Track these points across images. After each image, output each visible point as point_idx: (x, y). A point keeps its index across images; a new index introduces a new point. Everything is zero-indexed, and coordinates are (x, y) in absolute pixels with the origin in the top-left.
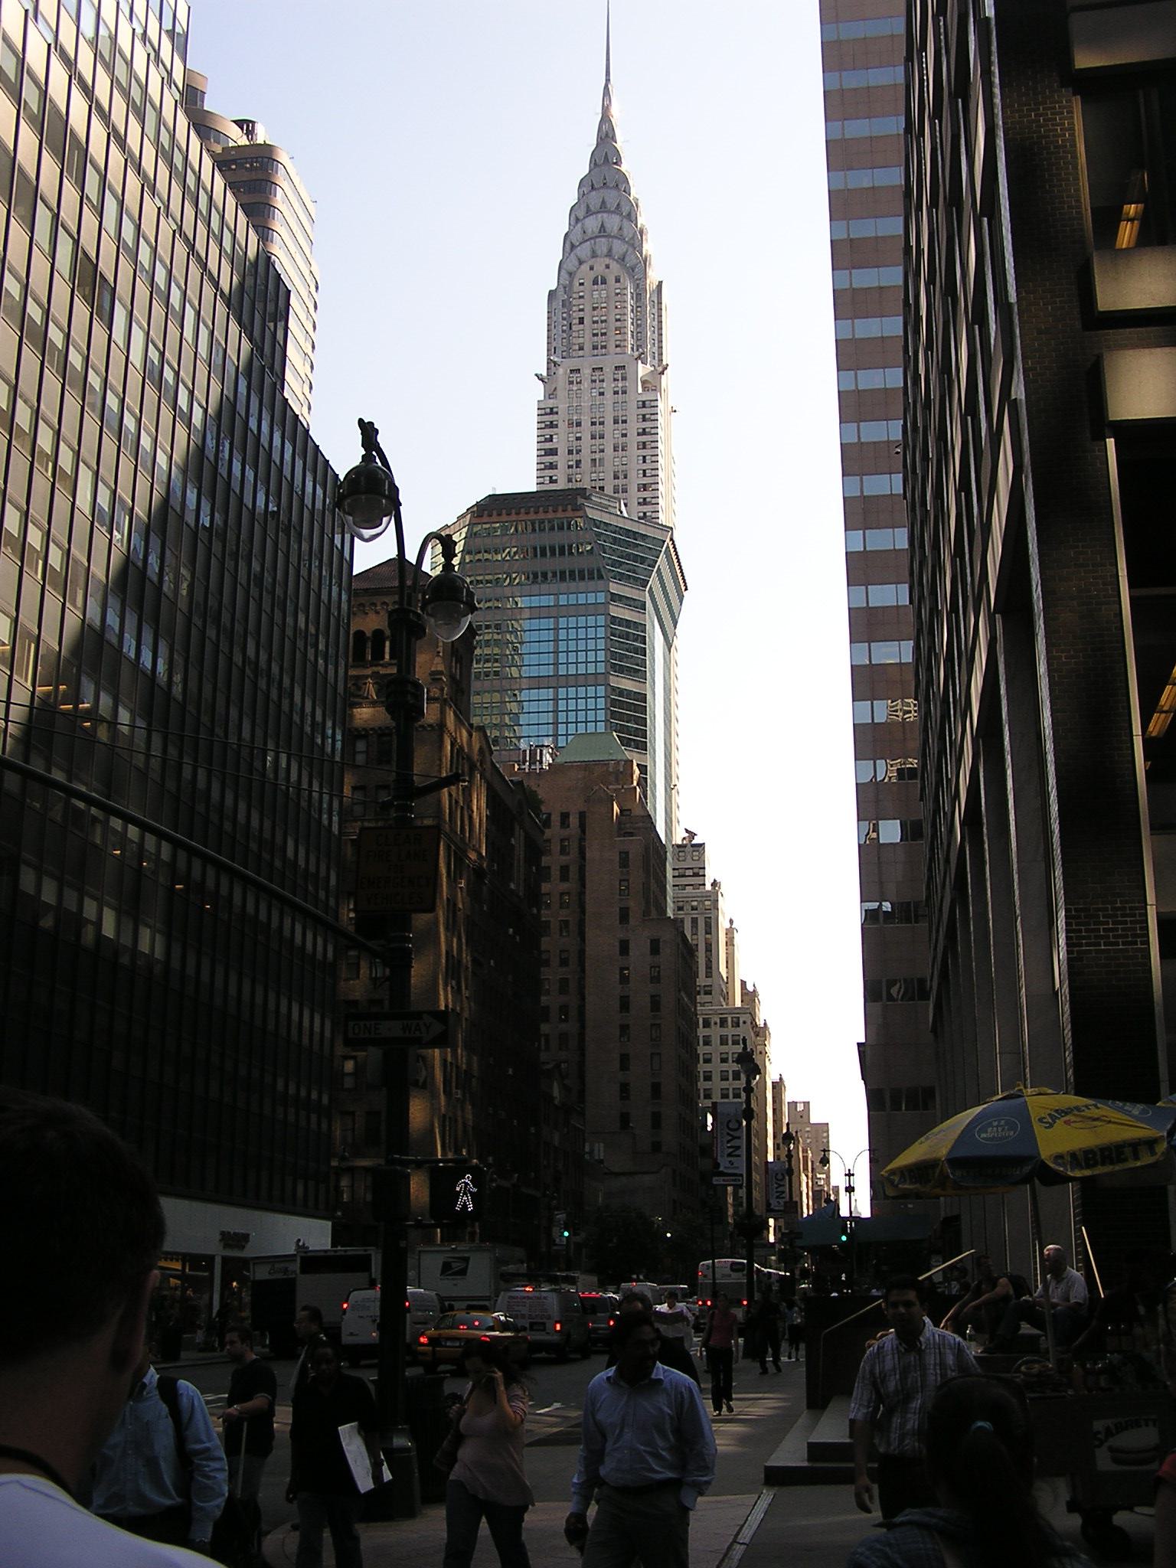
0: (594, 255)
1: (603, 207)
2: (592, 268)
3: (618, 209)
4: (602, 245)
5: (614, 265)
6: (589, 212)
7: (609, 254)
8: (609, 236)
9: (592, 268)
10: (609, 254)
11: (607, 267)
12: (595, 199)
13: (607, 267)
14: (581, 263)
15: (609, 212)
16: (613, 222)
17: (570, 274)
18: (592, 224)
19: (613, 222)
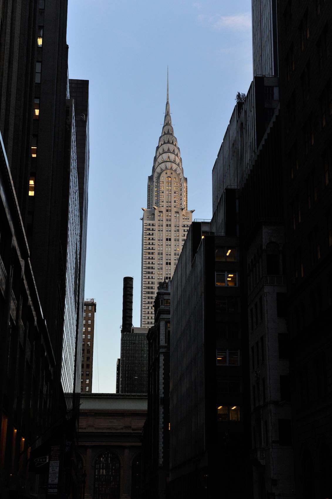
1: (169, 151)
2: (166, 173)
3: (173, 153)
4: (169, 165)
6: (164, 152)
8: (171, 162)
9: (166, 173)
10: (171, 169)
11: (172, 173)
12: (166, 147)
13: (172, 173)
14: (162, 171)
15: (170, 152)
17: (158, 173)
18: (165, 156)
19: (172, 157)
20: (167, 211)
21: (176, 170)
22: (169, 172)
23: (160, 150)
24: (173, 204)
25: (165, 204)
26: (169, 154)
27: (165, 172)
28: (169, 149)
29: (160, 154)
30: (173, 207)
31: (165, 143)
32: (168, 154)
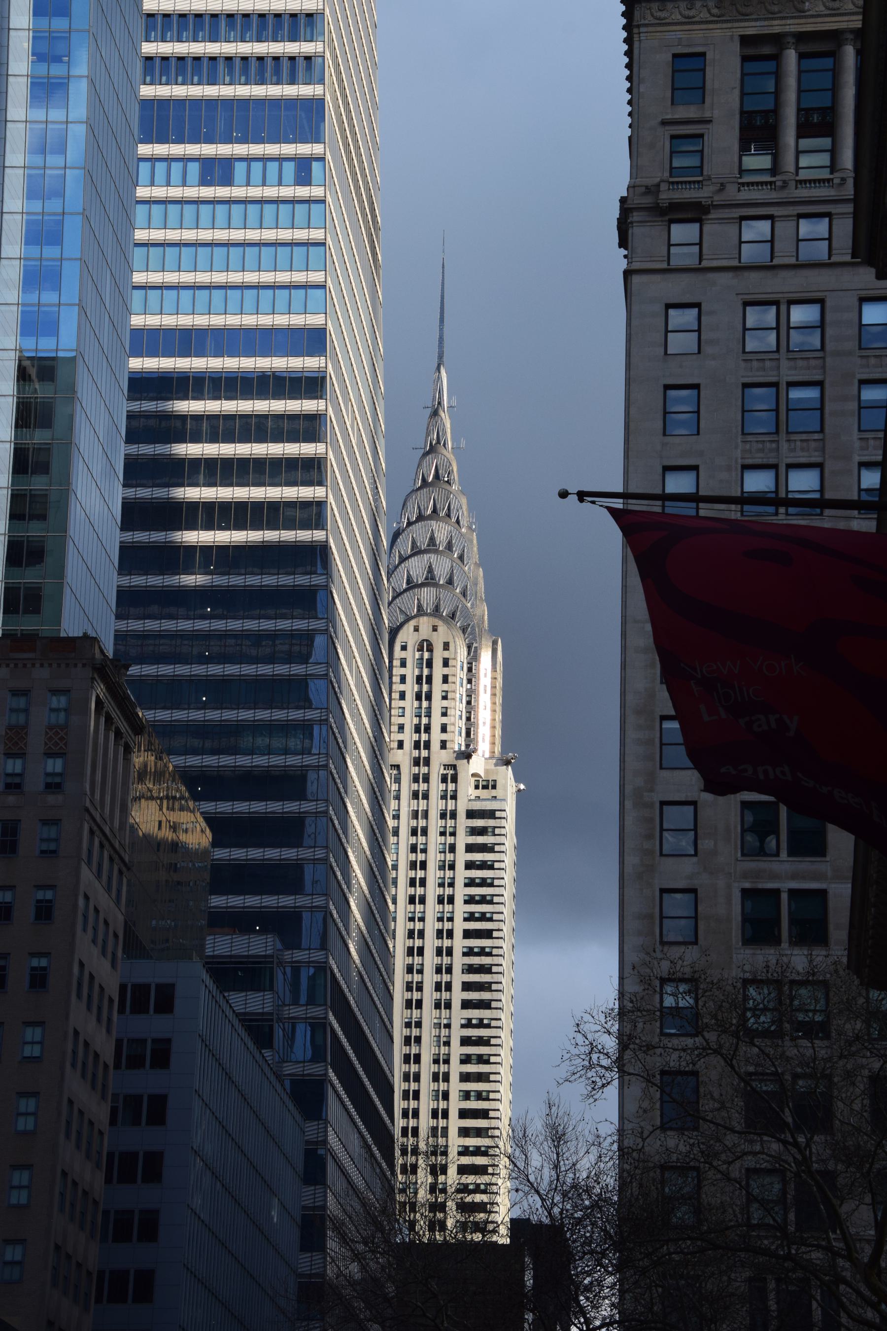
0: (421, 612)
2: (416, 629)
4: (427, 595)
5: (442, 628)
7: (436, 611)
9: (416, 629)
10: (437, 608)
11: (435, 629)
13: (435, 629)
15: (436, 551)
16: (442, 566)
18: (416, 567)
20: (416, 762)
21: (453, 616)
22: (425, 623)
23: (405, 546)
24: (436, 736)
25: (409, 737)
26: (433, 557)
27: (412, 623)
28: (432, 539)
29: (403, 559)
30: (435, 745)
31: (421, 518)
32: (426, 557)
